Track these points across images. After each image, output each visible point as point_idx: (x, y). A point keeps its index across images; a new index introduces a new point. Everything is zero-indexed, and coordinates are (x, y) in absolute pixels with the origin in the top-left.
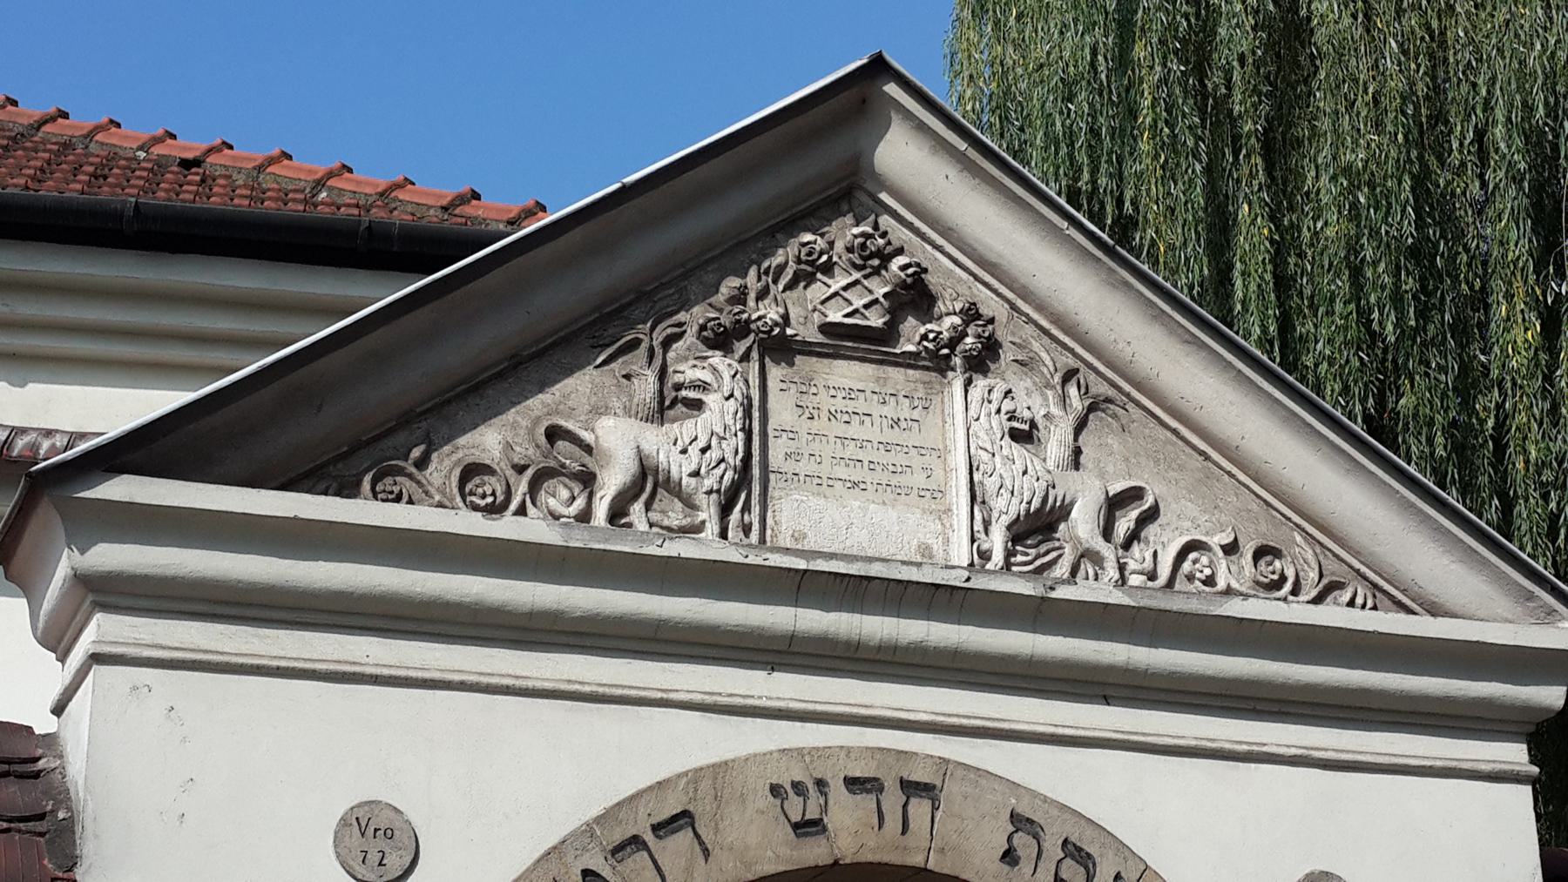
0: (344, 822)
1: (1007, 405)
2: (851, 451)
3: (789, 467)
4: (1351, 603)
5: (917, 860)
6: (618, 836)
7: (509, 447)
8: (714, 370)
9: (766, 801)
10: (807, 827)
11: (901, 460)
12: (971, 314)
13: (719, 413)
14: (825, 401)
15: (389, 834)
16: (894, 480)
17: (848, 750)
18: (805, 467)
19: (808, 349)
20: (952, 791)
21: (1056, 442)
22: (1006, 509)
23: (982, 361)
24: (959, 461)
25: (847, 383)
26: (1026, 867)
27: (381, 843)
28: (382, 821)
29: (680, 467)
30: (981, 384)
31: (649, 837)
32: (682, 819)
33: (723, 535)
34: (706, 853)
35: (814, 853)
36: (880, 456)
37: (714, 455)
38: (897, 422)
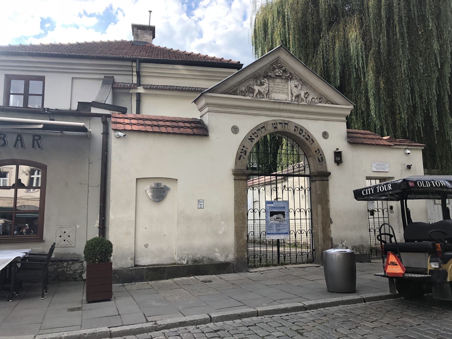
0: (232, 128)
1: (294, 83)
2: (279, 89)
3: (273, 91)
4: (329, 104)
5: (286, 131)
6: (258, 129)
7: (245, 89)
8: (265, 80)
9: (271, 125)
11: (283, 89)
12: (290, 73)
14: (276, 83)
15: (236, 129)
16: (283, 92)
17: (279, 120)
18: (274, 91)
19: (274, 78)
20: (289, 123)
21: (299, 88)
22: (295, 94)
23: (291, 79)
24: (290, 89)
25: (278, 81)
26: (296, 131)
28: (236, 127)
29: (262, 91)
30: (292, 81)
31: (260, 129)
32: (264, 127)
33: (266, 98)
35: (276, 130)
37: (265, 90)
38: (283, 85)
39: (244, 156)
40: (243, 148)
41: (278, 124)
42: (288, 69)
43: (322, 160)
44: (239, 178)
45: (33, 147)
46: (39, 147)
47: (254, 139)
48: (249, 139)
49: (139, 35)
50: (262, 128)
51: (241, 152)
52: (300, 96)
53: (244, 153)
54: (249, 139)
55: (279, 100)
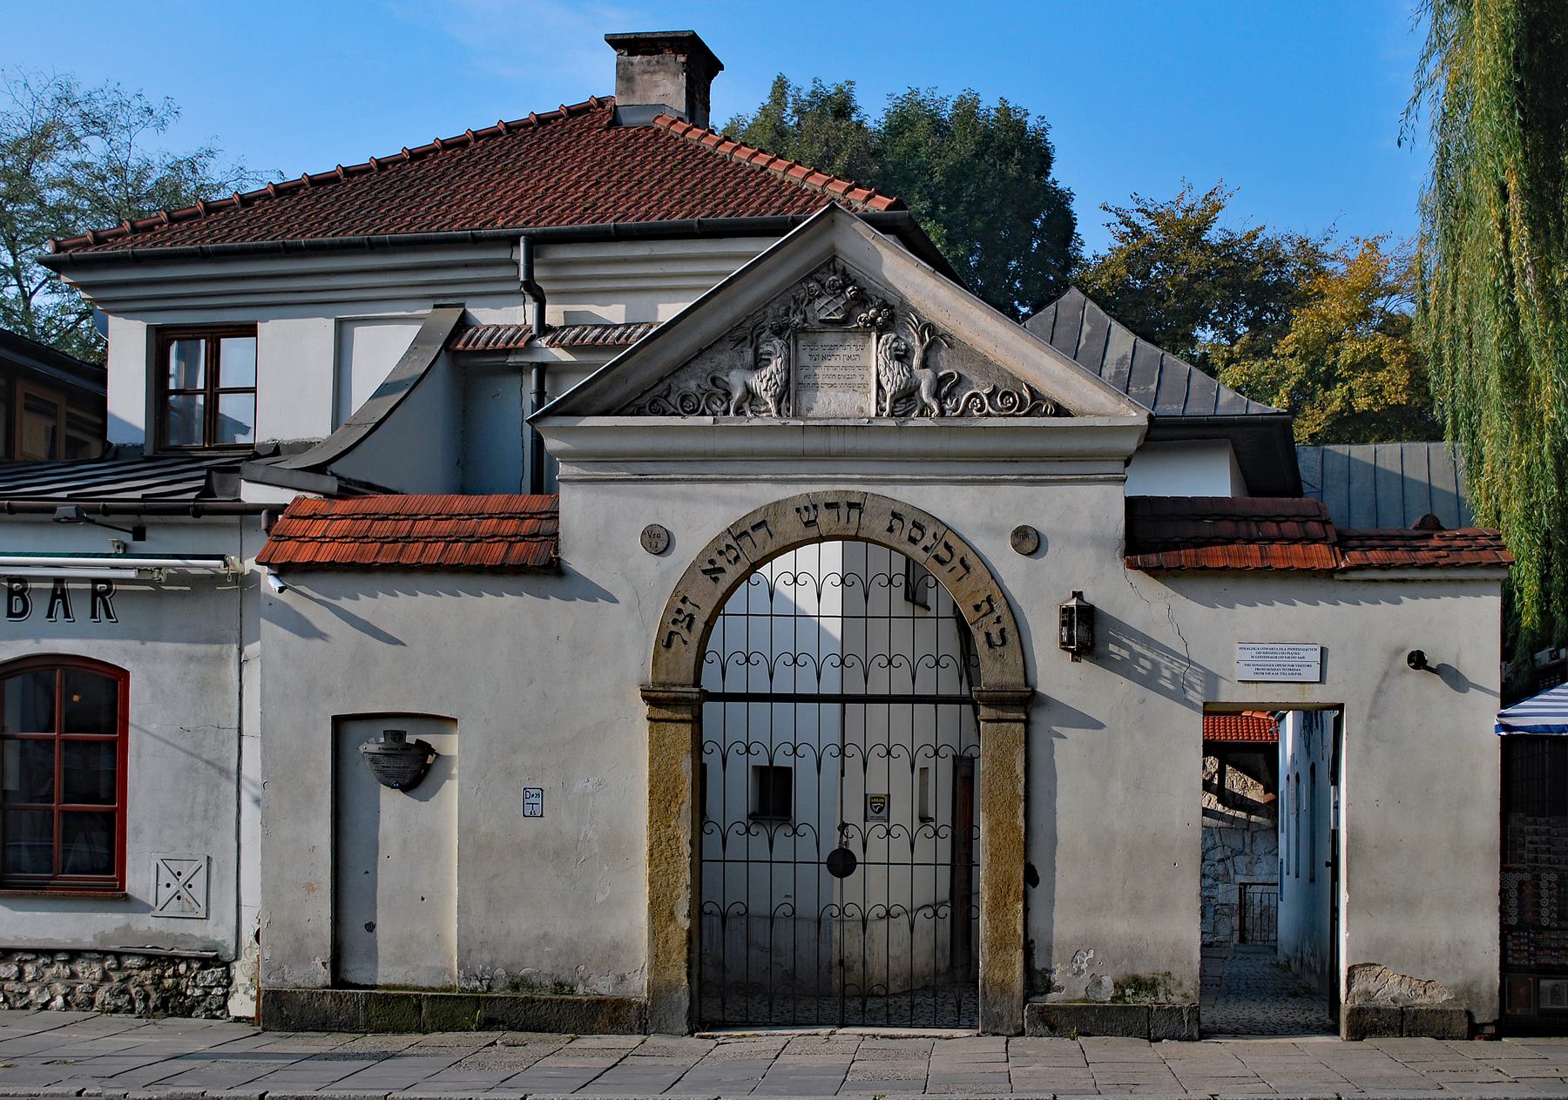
0: (643, 533)
2: (831, 371)
9: (792, 515)
10: (808, 524)
11: (852, 373)
13: (776, 364)
25: (830, 343)
27: (657, 540)
31: (750, 531)
32: (762, 524)
33: (779, 412)
34: (771, 535)
36: (844, 372)
39: (684, 633)
40: (680, 606)
41: (821, 508)
42: (876, 288)
43: (1013, 633)
44: (665, 713)
45: (94, 616)
46: (109, 616)
47: (722, 570)
48: (705, 572)
49: (638, 78)
50: (753, 528)
51: (675, 622)
52: (916, 394)
53: (684, 625)
54: (705, 572)
55: (820, 419)
